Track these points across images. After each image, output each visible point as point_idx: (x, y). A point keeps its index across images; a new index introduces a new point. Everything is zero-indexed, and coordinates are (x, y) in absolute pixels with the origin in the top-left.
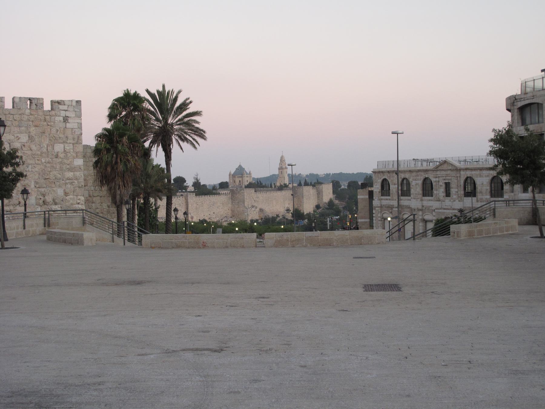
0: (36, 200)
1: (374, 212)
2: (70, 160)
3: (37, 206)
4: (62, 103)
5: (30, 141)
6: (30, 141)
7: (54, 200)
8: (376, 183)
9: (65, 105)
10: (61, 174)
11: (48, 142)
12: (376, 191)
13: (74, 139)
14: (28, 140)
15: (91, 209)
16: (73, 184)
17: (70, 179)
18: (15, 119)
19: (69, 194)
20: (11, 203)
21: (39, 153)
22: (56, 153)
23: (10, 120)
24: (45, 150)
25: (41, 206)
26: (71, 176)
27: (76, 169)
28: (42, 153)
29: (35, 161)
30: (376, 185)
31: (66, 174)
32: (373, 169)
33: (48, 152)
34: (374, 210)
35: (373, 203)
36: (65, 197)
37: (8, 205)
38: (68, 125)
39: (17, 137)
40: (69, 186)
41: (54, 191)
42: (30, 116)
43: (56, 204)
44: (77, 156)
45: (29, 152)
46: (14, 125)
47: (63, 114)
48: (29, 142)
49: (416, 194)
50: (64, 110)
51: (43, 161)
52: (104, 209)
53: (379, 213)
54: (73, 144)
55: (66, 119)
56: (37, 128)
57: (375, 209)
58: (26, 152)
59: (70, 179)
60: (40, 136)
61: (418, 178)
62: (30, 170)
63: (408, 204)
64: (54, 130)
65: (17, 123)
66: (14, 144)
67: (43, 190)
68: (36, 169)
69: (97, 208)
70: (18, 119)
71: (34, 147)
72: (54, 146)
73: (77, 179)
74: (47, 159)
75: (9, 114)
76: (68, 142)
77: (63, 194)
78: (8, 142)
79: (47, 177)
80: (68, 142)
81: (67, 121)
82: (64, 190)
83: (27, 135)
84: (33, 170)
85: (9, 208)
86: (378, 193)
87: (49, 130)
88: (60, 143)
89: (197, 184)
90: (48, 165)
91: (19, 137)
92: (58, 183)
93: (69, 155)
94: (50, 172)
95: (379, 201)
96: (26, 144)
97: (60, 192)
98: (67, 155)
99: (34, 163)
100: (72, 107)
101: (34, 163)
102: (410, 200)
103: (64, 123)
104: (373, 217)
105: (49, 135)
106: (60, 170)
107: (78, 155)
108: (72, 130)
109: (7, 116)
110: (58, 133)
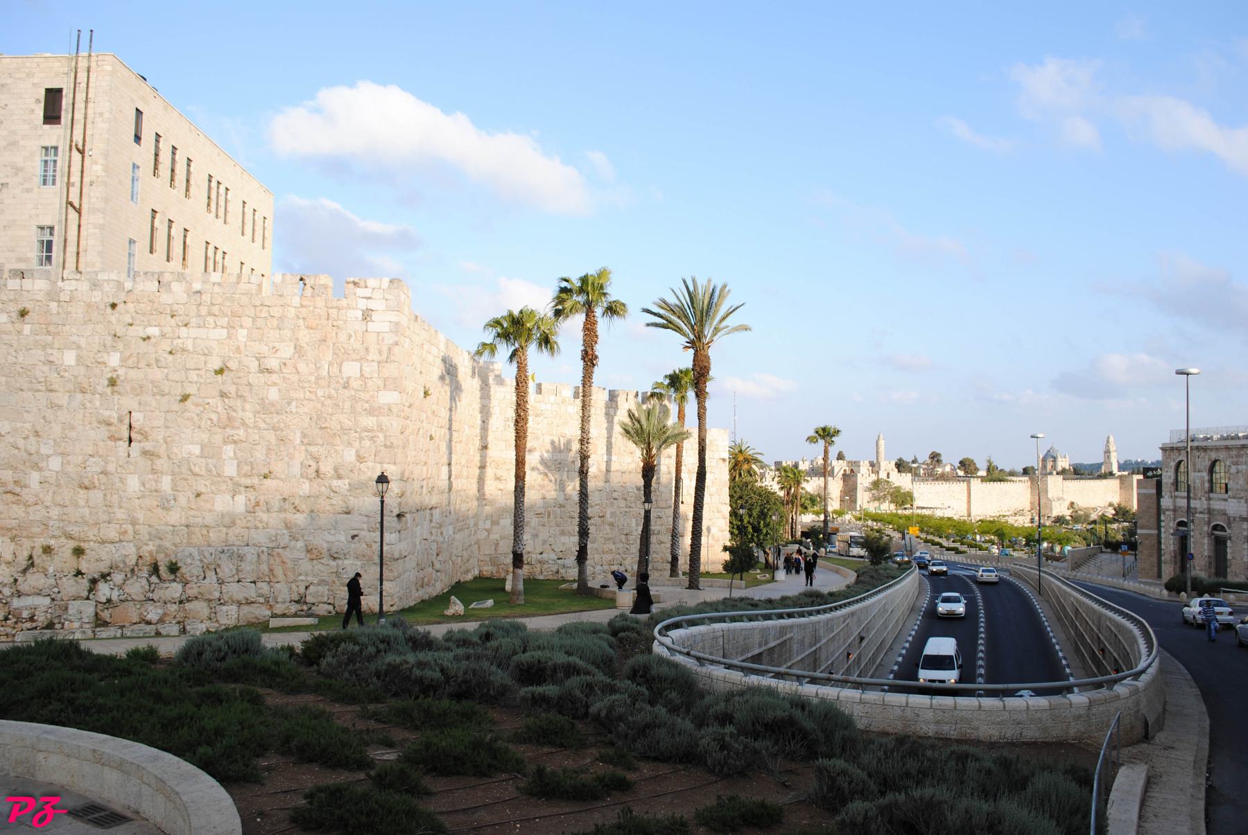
0: (301, 469)
1: (1162, 518)
2: (371, 393)
3: (302, 480)
4: (362, 284)
5: (297, 355)
6: (297, 355)
7: (336, 470)
9: (366, 287)
10: (353, 419)
11: (330, 359)
13: (380, 352)
14: (294, 353)
16: (375, 439)
17: (369, 431)
18: (272, 314)
19: (365, 460)
20: (254, 471)
21: (313, 379)
22: (345, 380)
23: (263, 316)
24: (325, 373)
25: (311, 480)
26: (371, 424)
27: (382, 411)
28: (318, 378)
29: (305, 393)
31: (361, 419)
33: (330, 377)
35: (1162, 504)
36: (358, 464)
37: (250, 476)
38: (371, 326)
39: (273, 348)
40: (367, 443)
41: (336, 451)
42: (300, 310)
43: (339, 477)
44: (385, 385)
45: (295, 378)
46: (269, 325)
47: (363, 304)
48: (296, 358)
49: (1237, 490)
50: (366, 298)
51: (320, 393)
54: (379, 362)
55: (367, 315)
56: (311, 331)
57: (1164, 513)
58: (287, 376)
59: (369, 431)
60: (316, 346)
61: (1240, 459)
62: (294, 411)
63: (1222, 508)
64: (343, 337)
65: (275, 323)
66: (266, 360)
67: (312, 449)
68: (306, 410)
70: (277, 315)
71: (302, 367)
72: (341, 365)
73: (381, 430)
74: (327, 390)
75: (262, 305)
76: (370, 358)
77: (353, 458)
78: (256, 358)
79: (323, 426)
80: (370, 358)
81: (369, 319)
82: (357, 451)
83: (292, 345)
84: (300, 411)
85: (250, 481)
86: (1169, 485)
87: (334, 335)
88: (353, 360)
89: (990, 469)
90: (329, 402)
91: (278, 347)
92: (346, 437)
93: (370, 383)
94: (332, 414)
95: (1171, 500)
96: (287, 362)
97: (350, 456)
98: (365, 384)
99: (302, 396)
100: (381, 291)
101: (302, 396)
102: (1226, 500)
103: (364, 322)
105: (334, 344)
106: (351, 413)
107: (387, 383)
108: (378, 336)
109: (257, 309)
110: (352, 340)
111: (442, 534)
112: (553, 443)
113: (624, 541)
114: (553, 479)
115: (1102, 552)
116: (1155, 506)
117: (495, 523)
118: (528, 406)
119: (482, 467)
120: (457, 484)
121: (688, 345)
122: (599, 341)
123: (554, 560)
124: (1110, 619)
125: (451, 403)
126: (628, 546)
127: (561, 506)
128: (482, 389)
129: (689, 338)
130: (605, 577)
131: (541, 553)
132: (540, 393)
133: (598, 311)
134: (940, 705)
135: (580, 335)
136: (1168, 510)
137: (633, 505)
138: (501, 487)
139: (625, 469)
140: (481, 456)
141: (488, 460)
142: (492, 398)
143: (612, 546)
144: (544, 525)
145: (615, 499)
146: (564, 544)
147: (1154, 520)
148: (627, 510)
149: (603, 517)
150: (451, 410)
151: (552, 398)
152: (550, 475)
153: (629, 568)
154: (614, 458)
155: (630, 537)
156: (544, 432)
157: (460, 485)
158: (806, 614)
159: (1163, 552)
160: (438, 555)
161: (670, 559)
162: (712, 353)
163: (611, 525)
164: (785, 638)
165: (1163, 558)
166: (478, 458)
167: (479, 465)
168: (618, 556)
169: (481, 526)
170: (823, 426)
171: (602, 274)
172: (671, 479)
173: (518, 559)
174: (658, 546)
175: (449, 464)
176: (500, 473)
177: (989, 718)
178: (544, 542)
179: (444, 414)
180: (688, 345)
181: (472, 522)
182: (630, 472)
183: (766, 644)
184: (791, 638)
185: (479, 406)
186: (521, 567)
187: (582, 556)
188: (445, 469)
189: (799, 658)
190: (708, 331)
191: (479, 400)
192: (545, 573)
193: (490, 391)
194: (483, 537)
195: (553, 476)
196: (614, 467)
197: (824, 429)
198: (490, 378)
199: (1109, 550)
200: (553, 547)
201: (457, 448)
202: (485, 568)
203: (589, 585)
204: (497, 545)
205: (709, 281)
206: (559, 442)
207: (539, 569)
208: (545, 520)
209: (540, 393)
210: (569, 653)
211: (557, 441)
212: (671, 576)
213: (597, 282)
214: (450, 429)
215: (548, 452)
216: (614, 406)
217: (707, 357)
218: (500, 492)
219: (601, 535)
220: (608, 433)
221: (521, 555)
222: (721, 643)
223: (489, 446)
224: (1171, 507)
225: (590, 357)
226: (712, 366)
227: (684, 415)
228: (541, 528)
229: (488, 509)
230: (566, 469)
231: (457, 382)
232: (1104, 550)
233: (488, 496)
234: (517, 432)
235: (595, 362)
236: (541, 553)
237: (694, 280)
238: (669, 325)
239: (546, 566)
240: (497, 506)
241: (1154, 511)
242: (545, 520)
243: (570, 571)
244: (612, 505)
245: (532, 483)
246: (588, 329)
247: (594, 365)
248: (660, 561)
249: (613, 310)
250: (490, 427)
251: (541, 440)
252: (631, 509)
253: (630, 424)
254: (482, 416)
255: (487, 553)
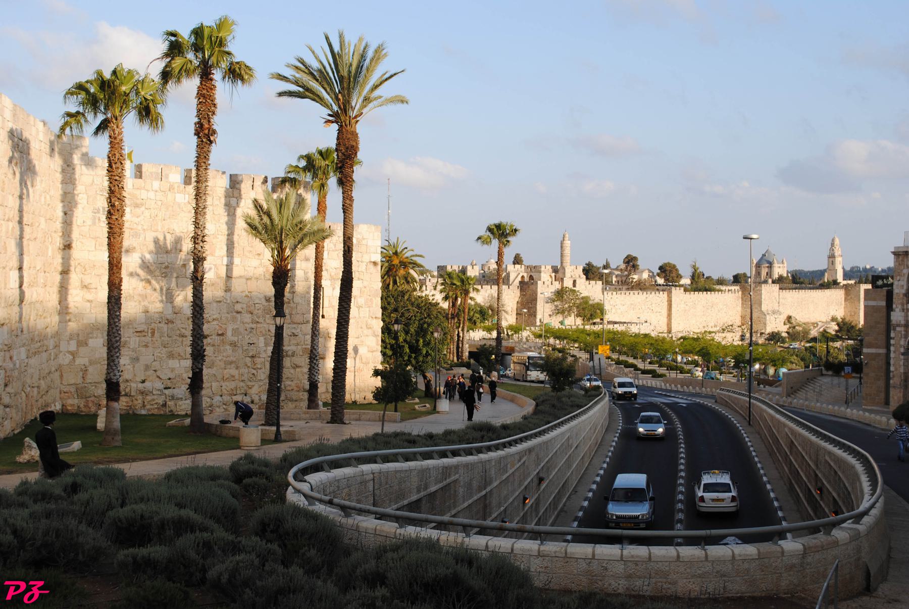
1: (892, 335)
8: (899, 275)
12: (897, 293)
15: (222, 303)
30: (899, 280)
32: (895, 248)
34: (892, 331)
35: (892, 318)
52: (256, 305)
53: (901, 337)
57: (894, 329)
69: (237, 302)
86: (901, 296)
104: (890, 345)
111: (11, 358)
112: (156, 241)
113: (249, 364)
114: (158, 287)
115: (822, 375)
116: (884, 321)
117: (82, 343)
118: (124, 194)
119: (65, 272)
120: (31, 294)
121: (331, 118)
122: (218, 111)
123: (159, 390)
124: (830, 453)
125: (22, 189)
126: (254, 371)
127: (169, 322)
128: (63, 171)
129: (331, 109)
130: (226, 410)
131: (143, 382)
132: (141, 177)
133: (217, 75)
134: (632, 556)
135: (193, 102)
136: (898, 325)
137: (261, 320)
138: (89, 296)
139: (251, 274)
140: (63, 258)
141: (72, 263)
142: (77, 182)
143: (234, 372)
144: (146, 346)
145: (238, 312)
146: (173, 370)
147: (883, 337)
148: (254, 326)
149: (222, 335)
150: (21, 197)
151: (156, 184)
152: (153, 282)
153: (256, 399)
154: (237, 261)
155: (258, 360)
156: (145, 227)
157: (35, 296)
158: (474, 452)
159: (891, 374)
160: (6, 385)
161: (307, 387)
162: (362, 129)
163: (234, 345)
164: (448, 481)
165: (891, 382)
166: (58, 260)
167: (60, 269)
168: (242, 384)
169: (63, 347)
170: (497, 222)
171: (222, 24)
172: (309, 288)
173: (113, 390)
174: (292, 371)
175: (20, 269)
176: (87, 280)
177: (688, 570)
178: (147, 368)
179: (13, 202)
180: (331, 118)
181: (51, 343)
182: (257, 279)
183: (426, 488)
184: (455, 481)
185: (60, 192)
186: (117, 400)
187: (196, 383)
188: (15, 275)
189: (466, 504)
190: (356, 101)
191: (60, 186)
192: (148, 407)
193: (74, 173)
194: (67, 361)
195: (158, 283)
196: (236, 272)
197: (498, 227)
198: (75, 157)
199: (830, 373)
200: (158, 373)
201: (30, 248)
202: (70, 402)
203: (205, 421)
204: (85, 371)
205: (361, 40)
206: (165, 238)
207: (140, 401)
208: (149, 339)
209: (141, 177)
210: (180, 506)
211: (161, 238)
212: (309, 407)
213: (215, 35)
214: (20, 222)
215: (150, 252)
216: (236, 193)
217: (355, 135)
218: (88, 304)
219: (220, 358)
220: (229, 229)
221: (117, 384)
222: (371, 489)
223: (74, 245)
224: (903, 322)
225: (206, 132)
226: (361, 146)
227: (326, 207)
228: (143, 349)
229: (73, 326)
230: (175, 275)
231: (30, 162)
232: (824, 372)
233: (72, 309)
234: (110, 226)
235: (212, 138)
236: (143, 382)
237: (341, 36)
238: (306, 93)
239: (149, 398)
240: (85, 322)
241: (882, 327)
242: (149, 339)
243: (180, 403)
244: (234, 319)
245: (131, 292)
246: (204, 96)
247: (211, 142)
248: (296, 389)
249: (236, 73)
250: (74, 219)
251: (142, 236)
252: (259, 325)
253: (257, 217)
254: (64, 206)
255: (73, 382)
